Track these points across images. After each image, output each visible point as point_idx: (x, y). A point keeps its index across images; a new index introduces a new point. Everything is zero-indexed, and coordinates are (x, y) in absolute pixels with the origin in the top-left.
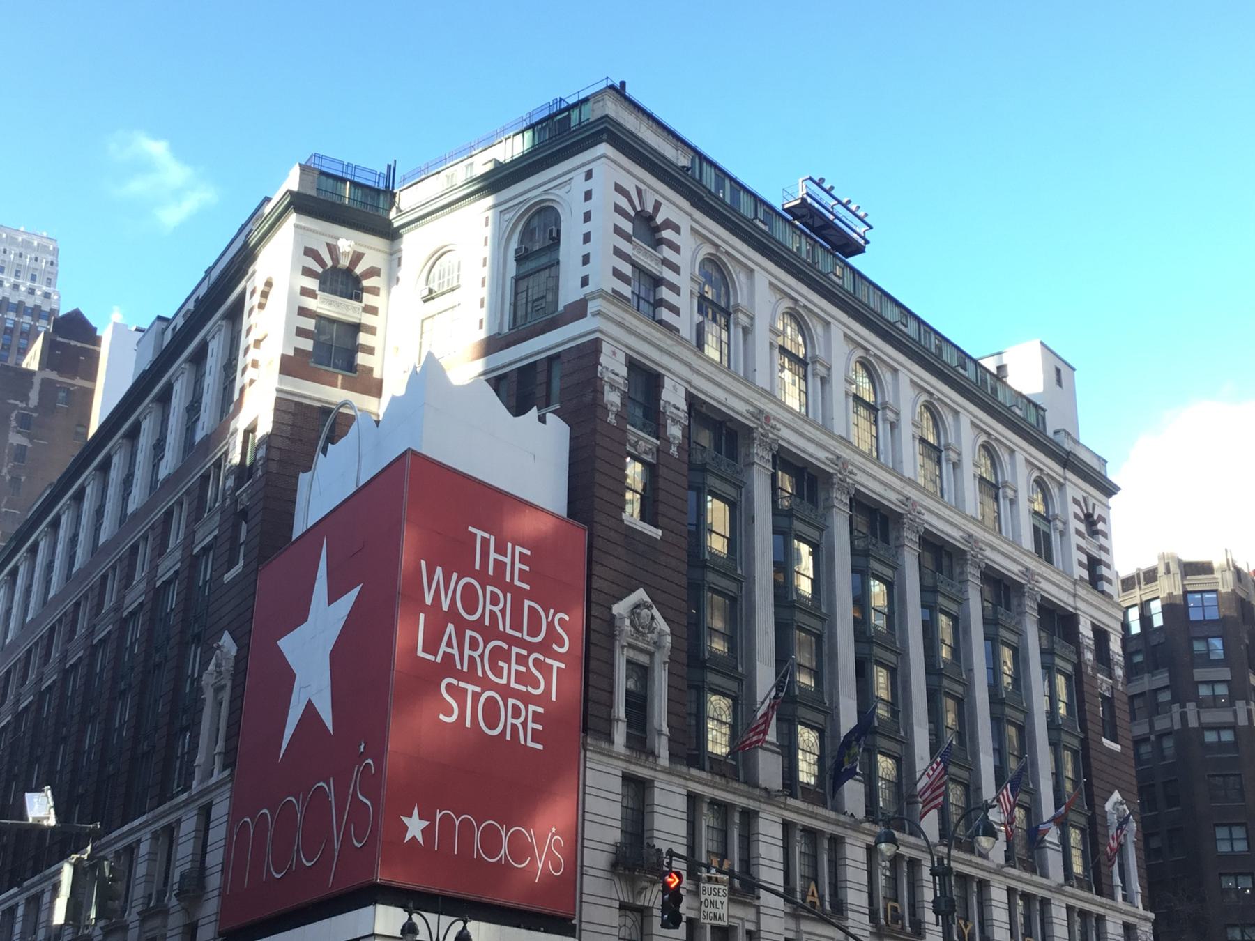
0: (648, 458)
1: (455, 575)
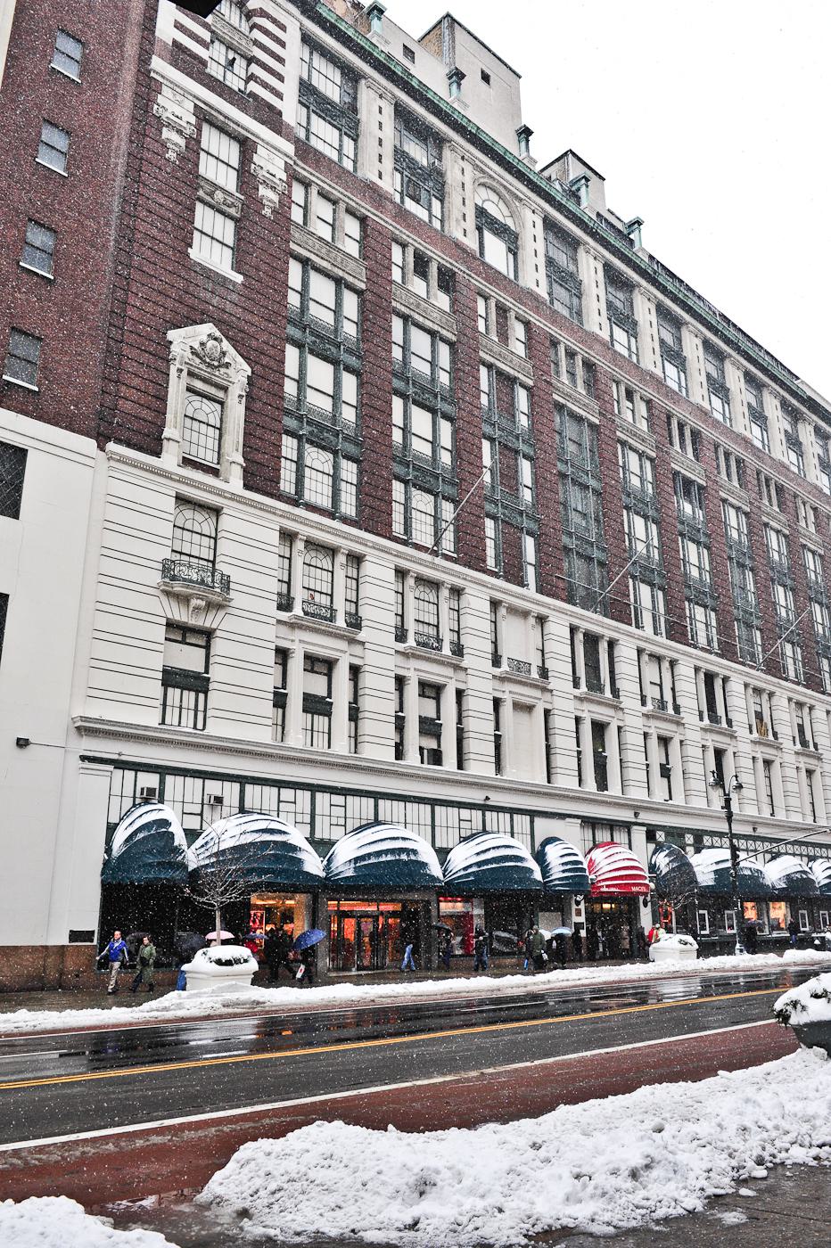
0: (232, 211)
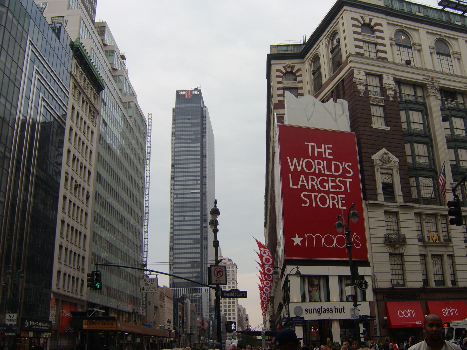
0: (381, 104)
1: (302, 159)
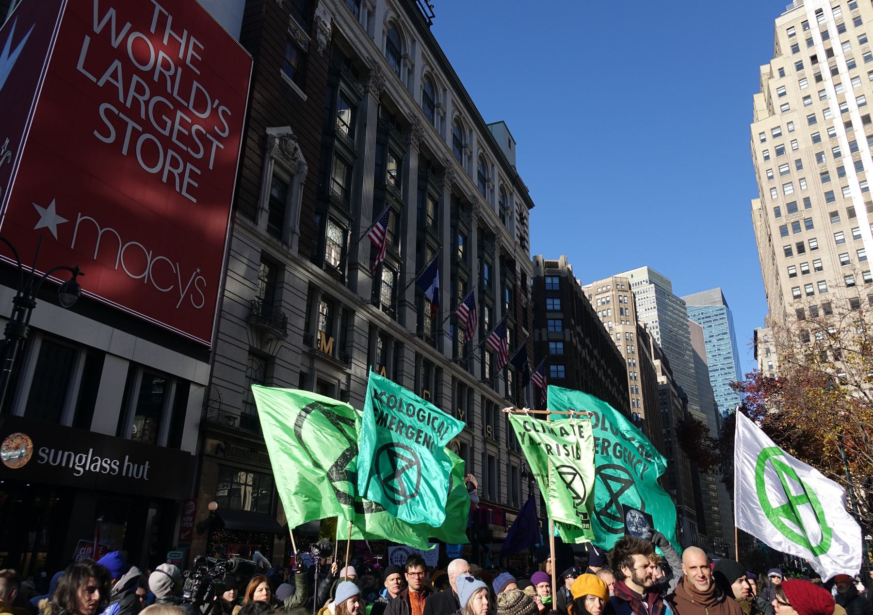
1: (128, 26)
